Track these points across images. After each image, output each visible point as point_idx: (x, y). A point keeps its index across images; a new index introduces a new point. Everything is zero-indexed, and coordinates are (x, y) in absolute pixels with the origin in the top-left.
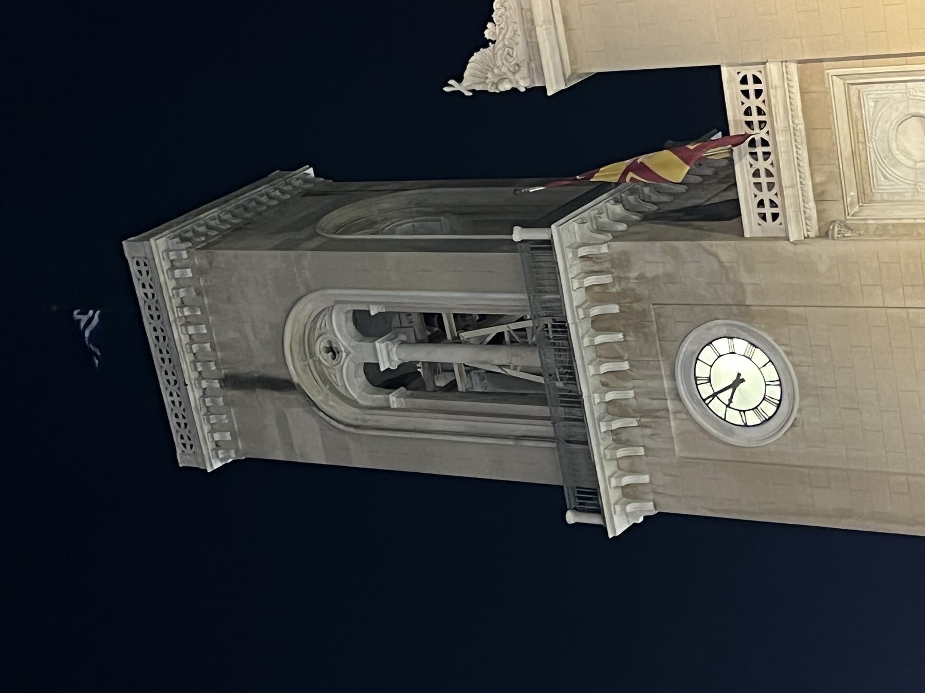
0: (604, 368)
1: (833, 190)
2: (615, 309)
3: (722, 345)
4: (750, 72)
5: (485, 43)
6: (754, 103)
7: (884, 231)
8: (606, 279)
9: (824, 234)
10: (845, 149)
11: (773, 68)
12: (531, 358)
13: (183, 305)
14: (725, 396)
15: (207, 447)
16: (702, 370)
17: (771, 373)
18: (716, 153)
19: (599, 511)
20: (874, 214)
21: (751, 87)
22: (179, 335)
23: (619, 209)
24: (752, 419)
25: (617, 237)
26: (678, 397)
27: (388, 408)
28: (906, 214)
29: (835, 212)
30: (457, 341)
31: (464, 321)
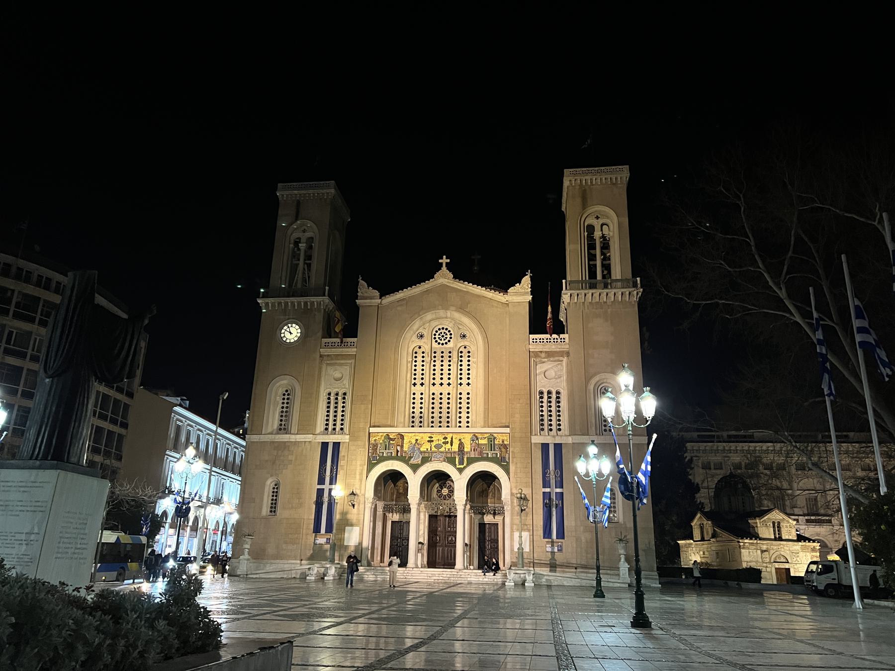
0: (296, 304)
1: (329, 358)
2: (309, 308)
3: (299, 331)
4: (355, 344)
5: (368, 287)
6: (349, 344)
7: (320, 369)
8: (316, 307)
9: (321, 356)
10: (338, 362)
11: (355, 349)
12: (299, 286)
13: (318, 194)
14: (288, 330)
15: (282, 193)
16: (294, 325)
17: (292, 341)
18: (340, 336)
19: (263, 297)
20: (324, 366)
21: (352, 344)
22: (311, 191)
23: (331, 308)
24: (282, 335)
25: (325, 310)
26: (288, 319)
27: (290, 244)
28: (323, 373)
29: (325, 358)
30: (305, 263)
31: (309, 265)
